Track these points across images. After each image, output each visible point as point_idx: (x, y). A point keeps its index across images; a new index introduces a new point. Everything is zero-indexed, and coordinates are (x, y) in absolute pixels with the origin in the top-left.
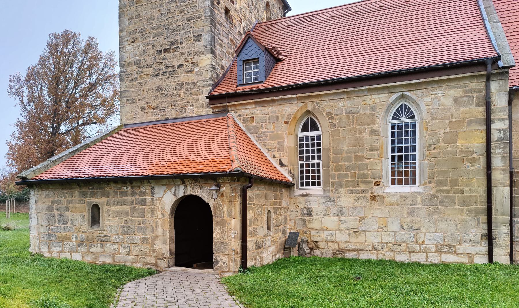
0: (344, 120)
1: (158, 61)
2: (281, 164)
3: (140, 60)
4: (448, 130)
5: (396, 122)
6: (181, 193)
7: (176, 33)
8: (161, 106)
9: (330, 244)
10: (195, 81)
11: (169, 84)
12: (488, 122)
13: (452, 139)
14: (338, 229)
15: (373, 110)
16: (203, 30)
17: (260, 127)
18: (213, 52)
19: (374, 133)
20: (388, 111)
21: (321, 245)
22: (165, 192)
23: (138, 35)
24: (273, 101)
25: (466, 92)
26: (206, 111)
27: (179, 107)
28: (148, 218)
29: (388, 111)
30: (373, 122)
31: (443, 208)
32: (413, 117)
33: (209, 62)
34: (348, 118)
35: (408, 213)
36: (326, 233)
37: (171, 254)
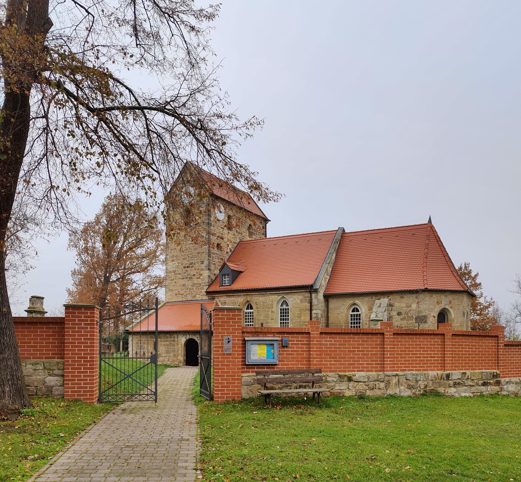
0: (262, 306)
1: (184, 272)
3: (175, 270)
4: (298, 313)
6: (188, 338)
8: (185, 294)
11: (189, 283)
12: (311, 310)
13: (299, 316)
15: (272, 302)
16: (205, 259)
18: (209, 269)
19: (272, 312)
20: (278, 303)
22: (182, 337)
23: (175, 258)
25: (304, 297)
26: (205, 297)
27: (193, 295)
28: (176, 346)
29: (278, 303)
30: (273, 308)
32: (288, 306)
33: (207, 274)
34: (263, 305)
37: (184, 361)
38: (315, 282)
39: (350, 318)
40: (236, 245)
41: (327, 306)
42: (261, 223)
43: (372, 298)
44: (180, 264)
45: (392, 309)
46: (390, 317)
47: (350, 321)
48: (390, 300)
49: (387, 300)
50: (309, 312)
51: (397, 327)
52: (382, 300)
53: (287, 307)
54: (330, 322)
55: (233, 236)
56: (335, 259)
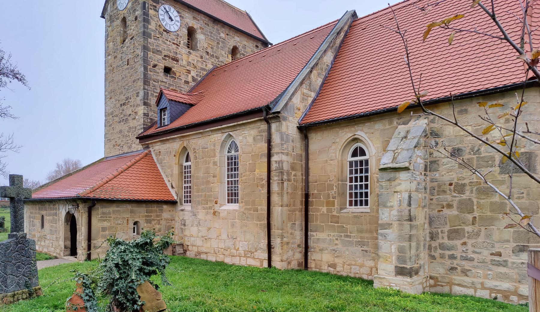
2: (172, 187)
4: (251, 162)
5: (230, 154)
7: (128, 91)
9: (194, 247)
10: (136, 126)
11: (124, 127)
12: (269, 156)
14: (198, 237)
17: (163, 159)
18: (145, 104)
19: (215, 163)
20: (222, 146)
21: (190, 248)
23: (113, 94)
24: (168, 140)
26: (140, 147)
31: (248, 222)
32: (238, 151)
35: (231, 226)
36: (192, 239)
38: (276, 101)
39: (348, 169)
40: (205, 73)
41: (307, 148)
42: (257, 46)
43: (391, 123)
44: (117, 101)
45: (437, 144)
46: (431, 162)
47: (348, 176)
48: (433, 121)
49: (426, 121)
50: (266, 160)
51: (451, 184)
52: (412, 123)
53: (236, 154)
54: (311, 178)
55: (200, 60)
56: (332, 64)
